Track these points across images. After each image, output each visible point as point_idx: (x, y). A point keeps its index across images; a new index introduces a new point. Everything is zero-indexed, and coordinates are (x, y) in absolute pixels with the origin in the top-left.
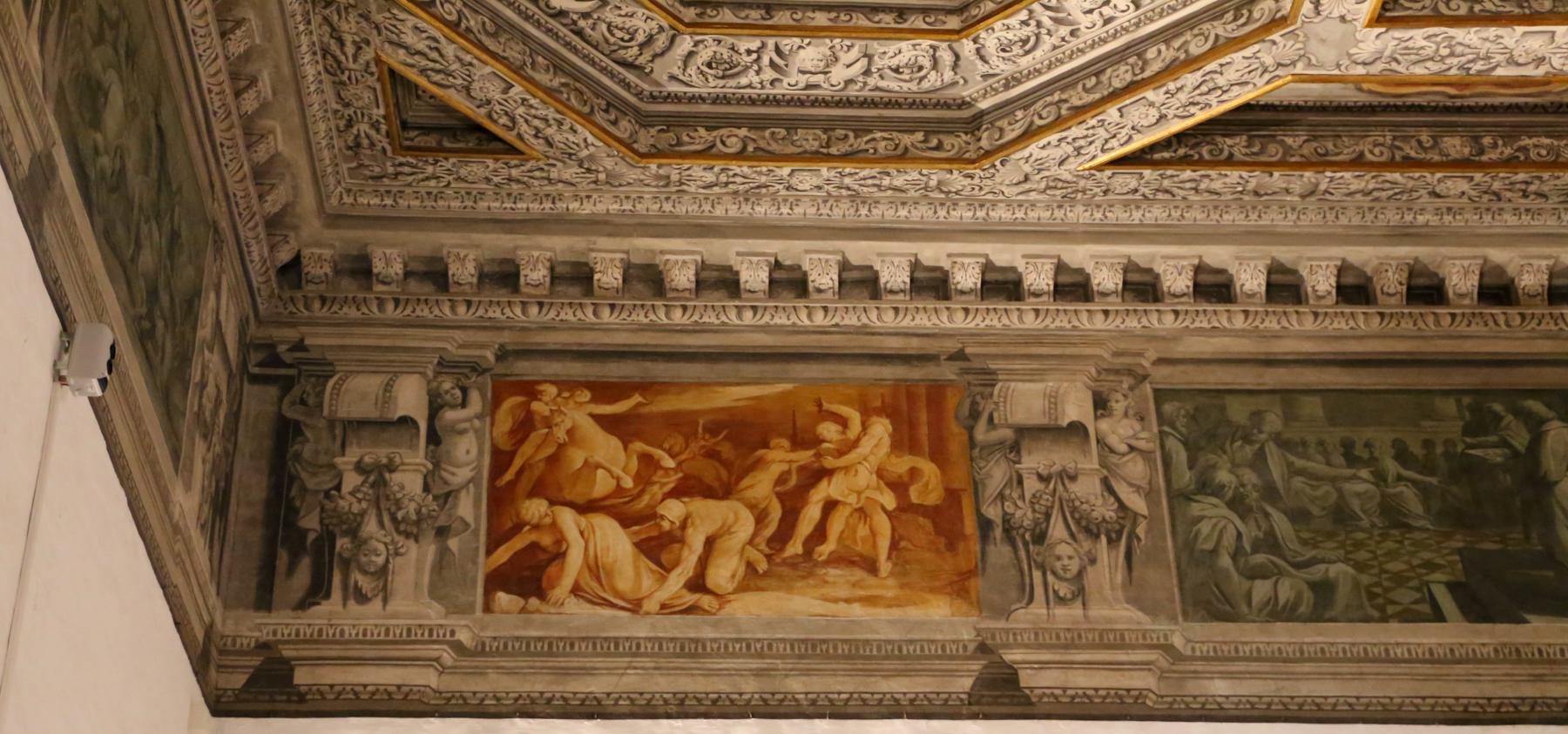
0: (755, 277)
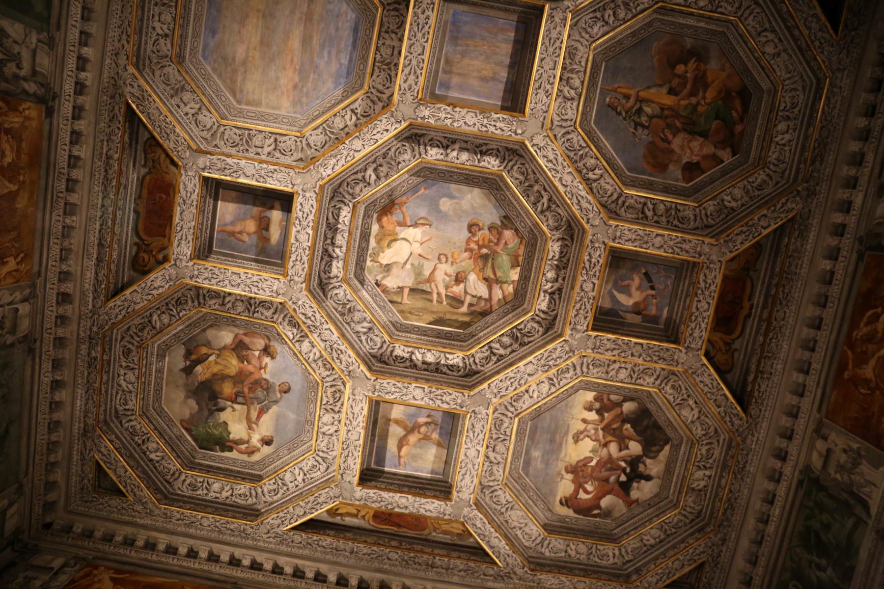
0: (183, 550)
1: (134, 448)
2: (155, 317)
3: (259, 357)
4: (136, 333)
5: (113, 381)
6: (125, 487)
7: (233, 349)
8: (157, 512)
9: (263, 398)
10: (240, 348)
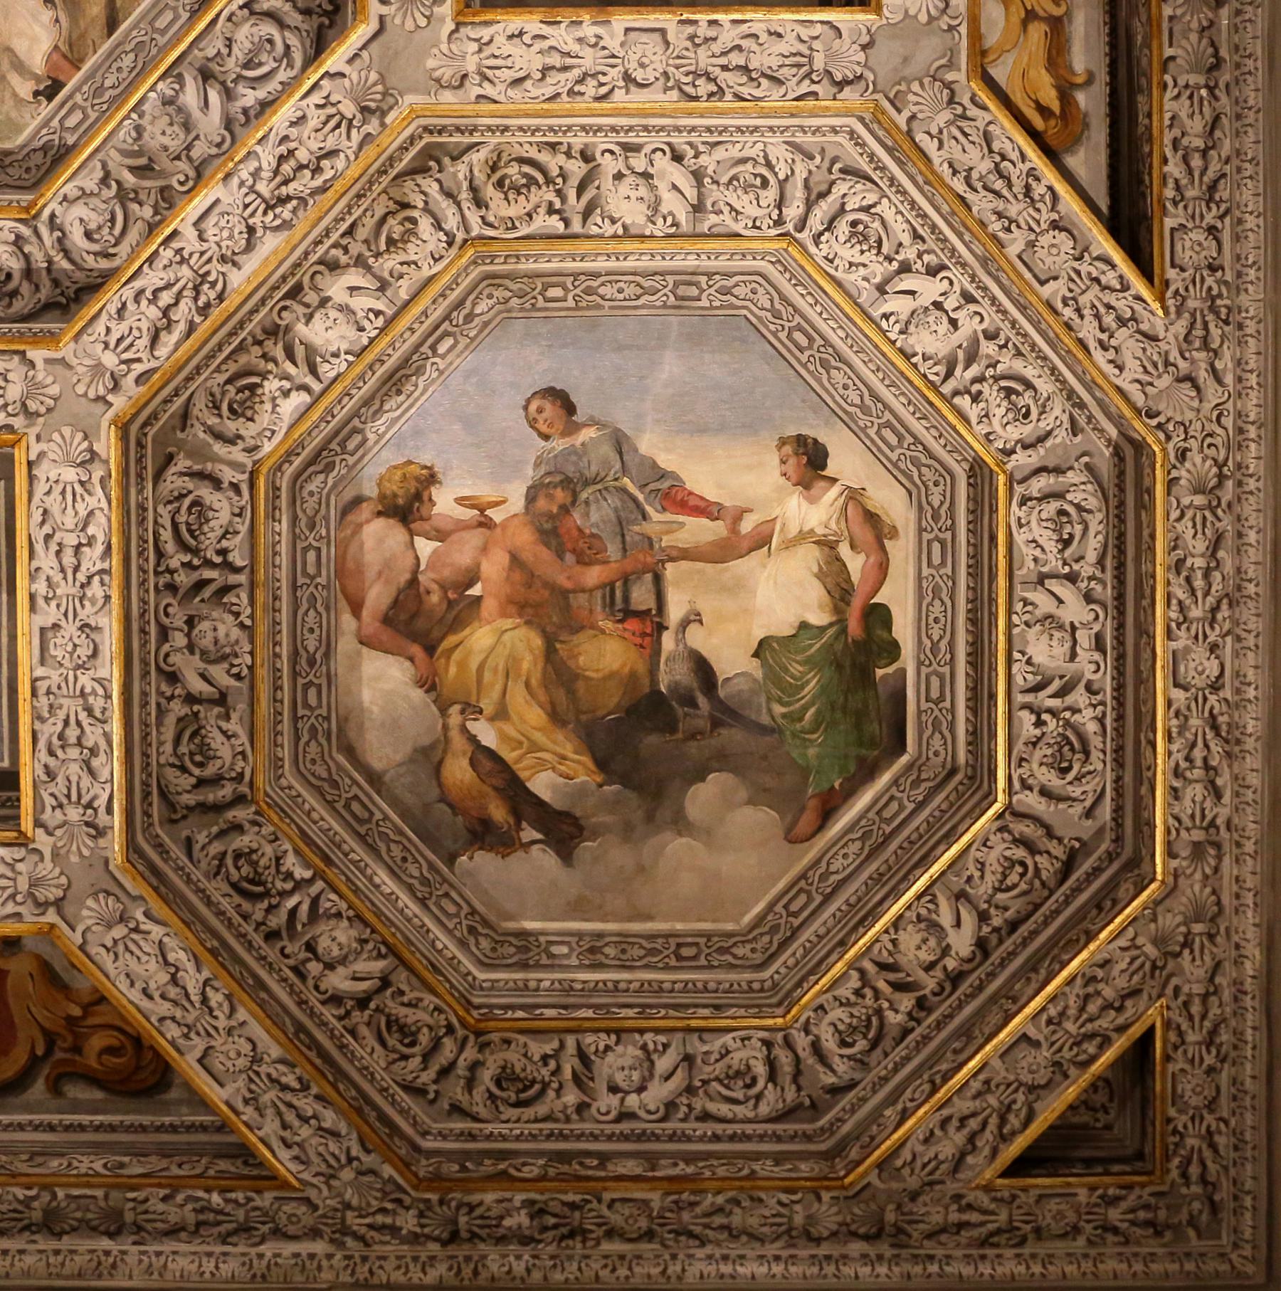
1: (939, 1026)
2: (339, 981)
3: (440, 535)
4: (426, 1058)
5: (657, 1138)
6: (1106, 1042)
7: (430, 650)
8: (1194, 888)
9: (614, 500)
10: (420, 622)
